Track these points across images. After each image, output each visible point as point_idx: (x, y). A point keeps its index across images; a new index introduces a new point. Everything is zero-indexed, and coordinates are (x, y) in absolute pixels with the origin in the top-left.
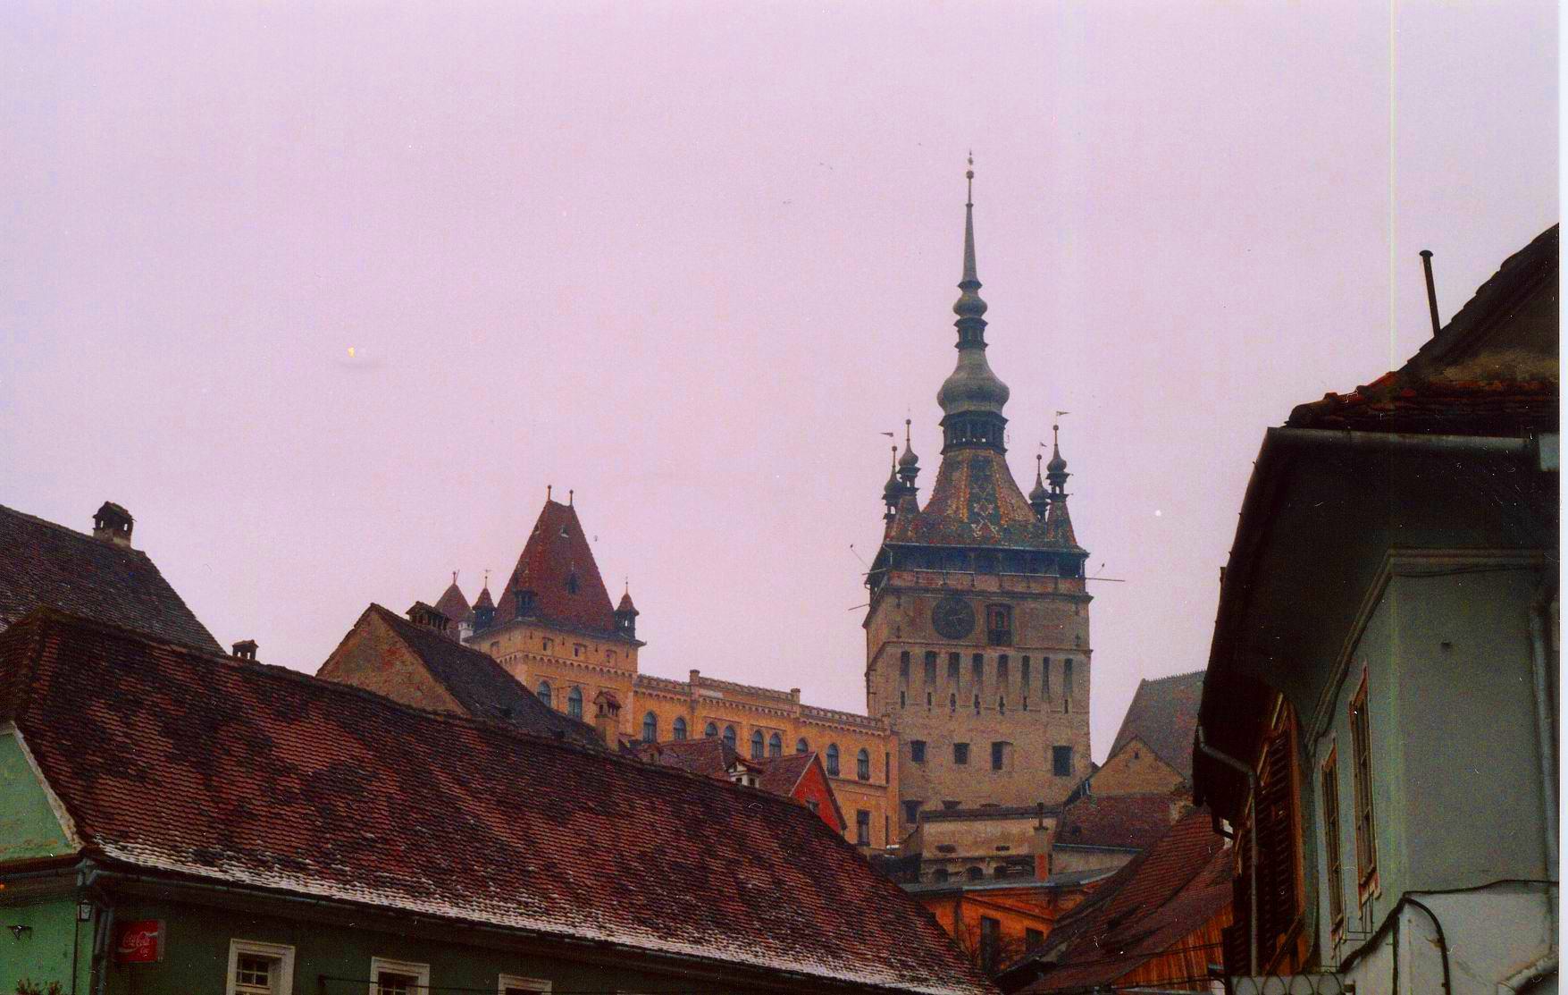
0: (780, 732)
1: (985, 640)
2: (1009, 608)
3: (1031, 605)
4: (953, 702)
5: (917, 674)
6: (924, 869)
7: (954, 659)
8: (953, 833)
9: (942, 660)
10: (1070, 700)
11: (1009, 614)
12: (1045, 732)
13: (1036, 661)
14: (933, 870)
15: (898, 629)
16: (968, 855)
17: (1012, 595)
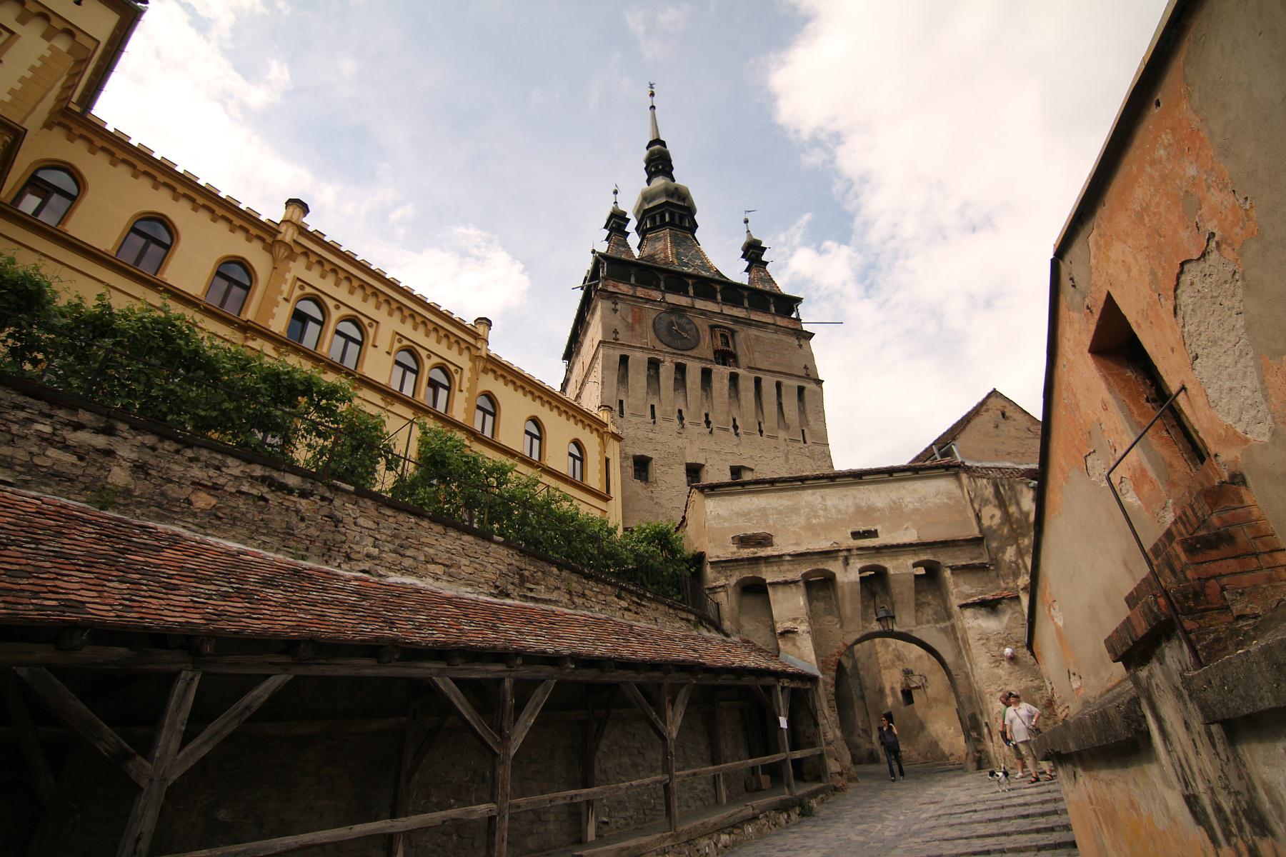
0: (452, 368)
1: (711, 356)
2: (733, 332)
3: (753, 332)
4: (681, 418)
5: (638, 377)
6: (716, 579)
7: (681, 369)
8: (763, 512)
9: (667, 371)
10: (806, 430)
11: (733, 335)
12: (787, 460)
13: (768, 384)
14: (733, 581)
15: (616, 332)
16: (802, 549)
17: (736, 320)
